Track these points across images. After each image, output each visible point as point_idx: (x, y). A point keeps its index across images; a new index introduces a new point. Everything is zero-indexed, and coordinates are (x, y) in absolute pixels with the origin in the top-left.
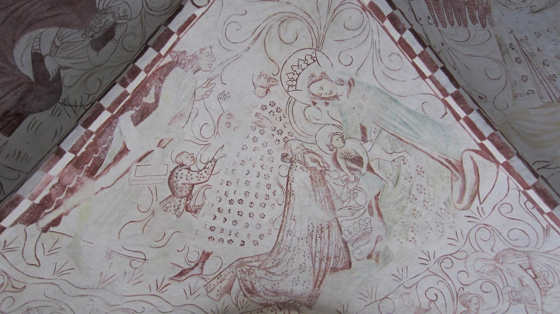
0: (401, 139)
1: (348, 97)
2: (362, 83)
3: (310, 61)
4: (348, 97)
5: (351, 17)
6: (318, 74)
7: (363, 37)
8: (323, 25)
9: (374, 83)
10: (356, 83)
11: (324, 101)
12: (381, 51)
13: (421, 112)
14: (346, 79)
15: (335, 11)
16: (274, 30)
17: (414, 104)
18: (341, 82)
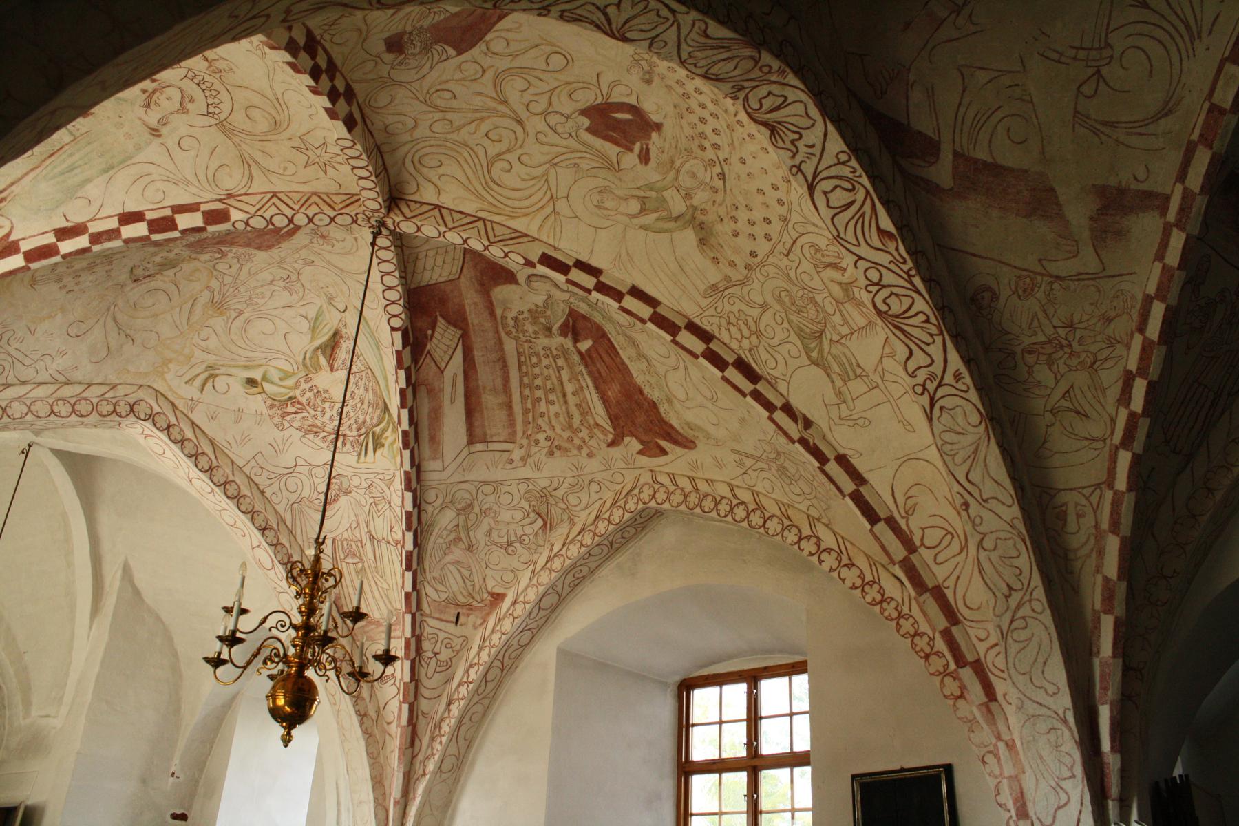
0: (51, 155)
1: (140, 119)
2: (148, 144)
3: (211, 109)
4: (140, 119)
5: (231, 176)
6: (189, 106)
7: (202, 177)
8: (243, 145)
9: (141, 157)
10: (152, 137)
11: (150, 90)
12: (174, 186)
13: (79, 194)
14: (164, 131)
15: (249, 165)
16: (273, 112)
17: (92, 190)
18: (163, 122)
